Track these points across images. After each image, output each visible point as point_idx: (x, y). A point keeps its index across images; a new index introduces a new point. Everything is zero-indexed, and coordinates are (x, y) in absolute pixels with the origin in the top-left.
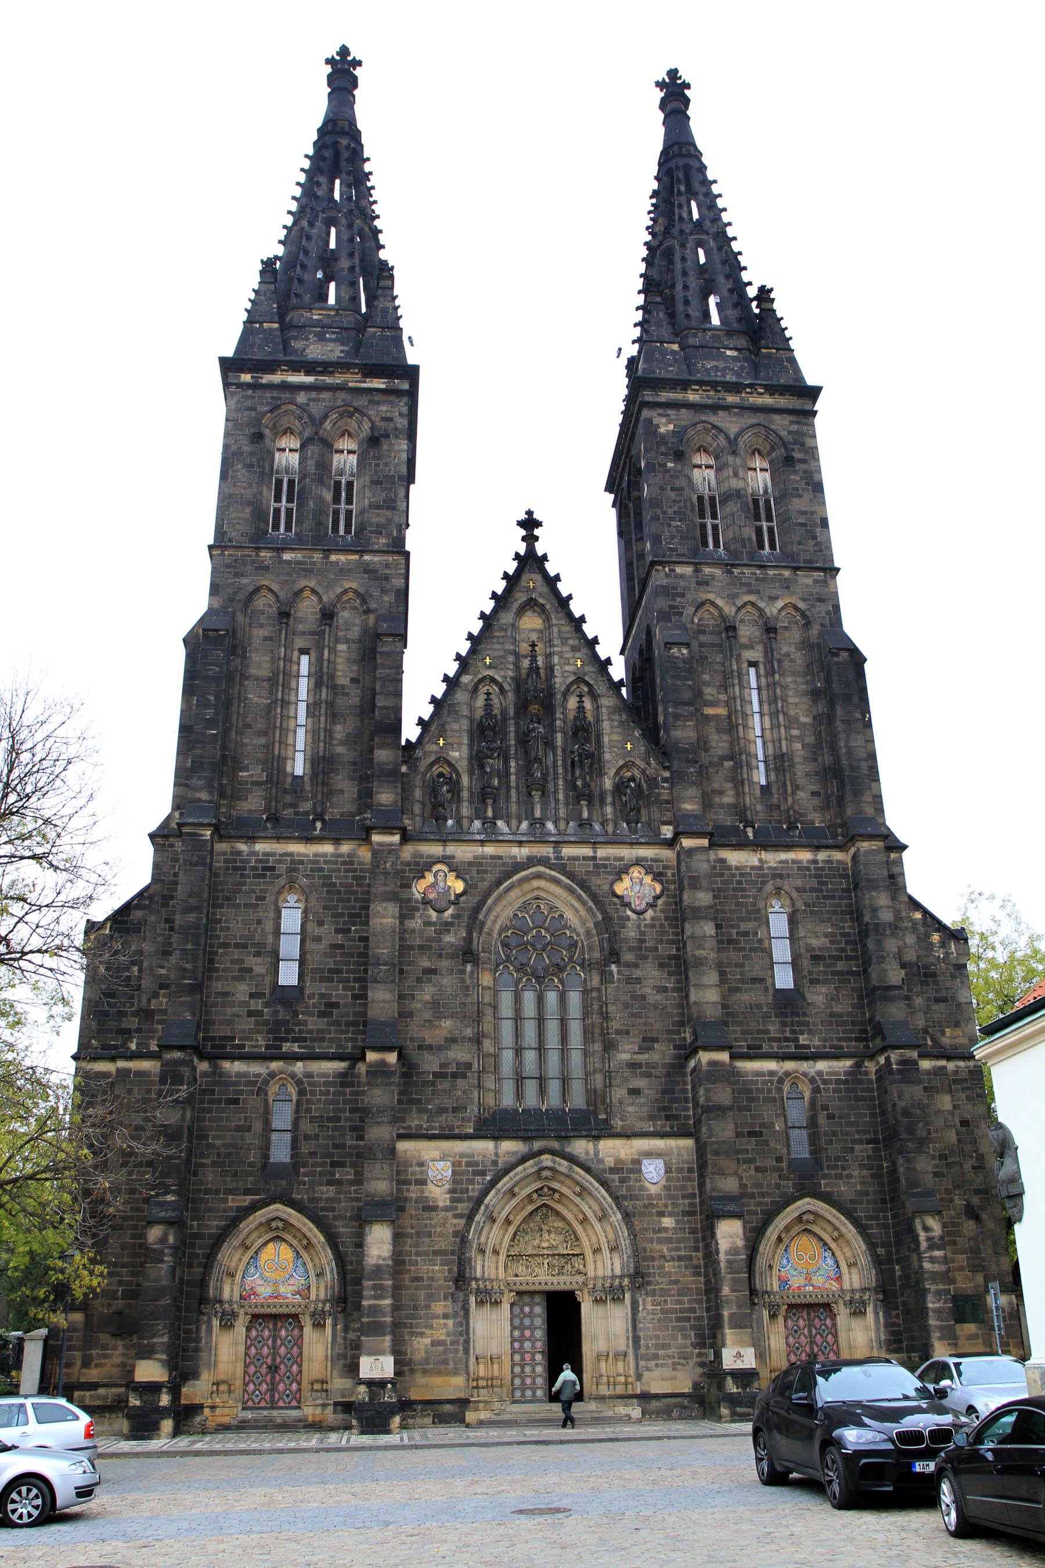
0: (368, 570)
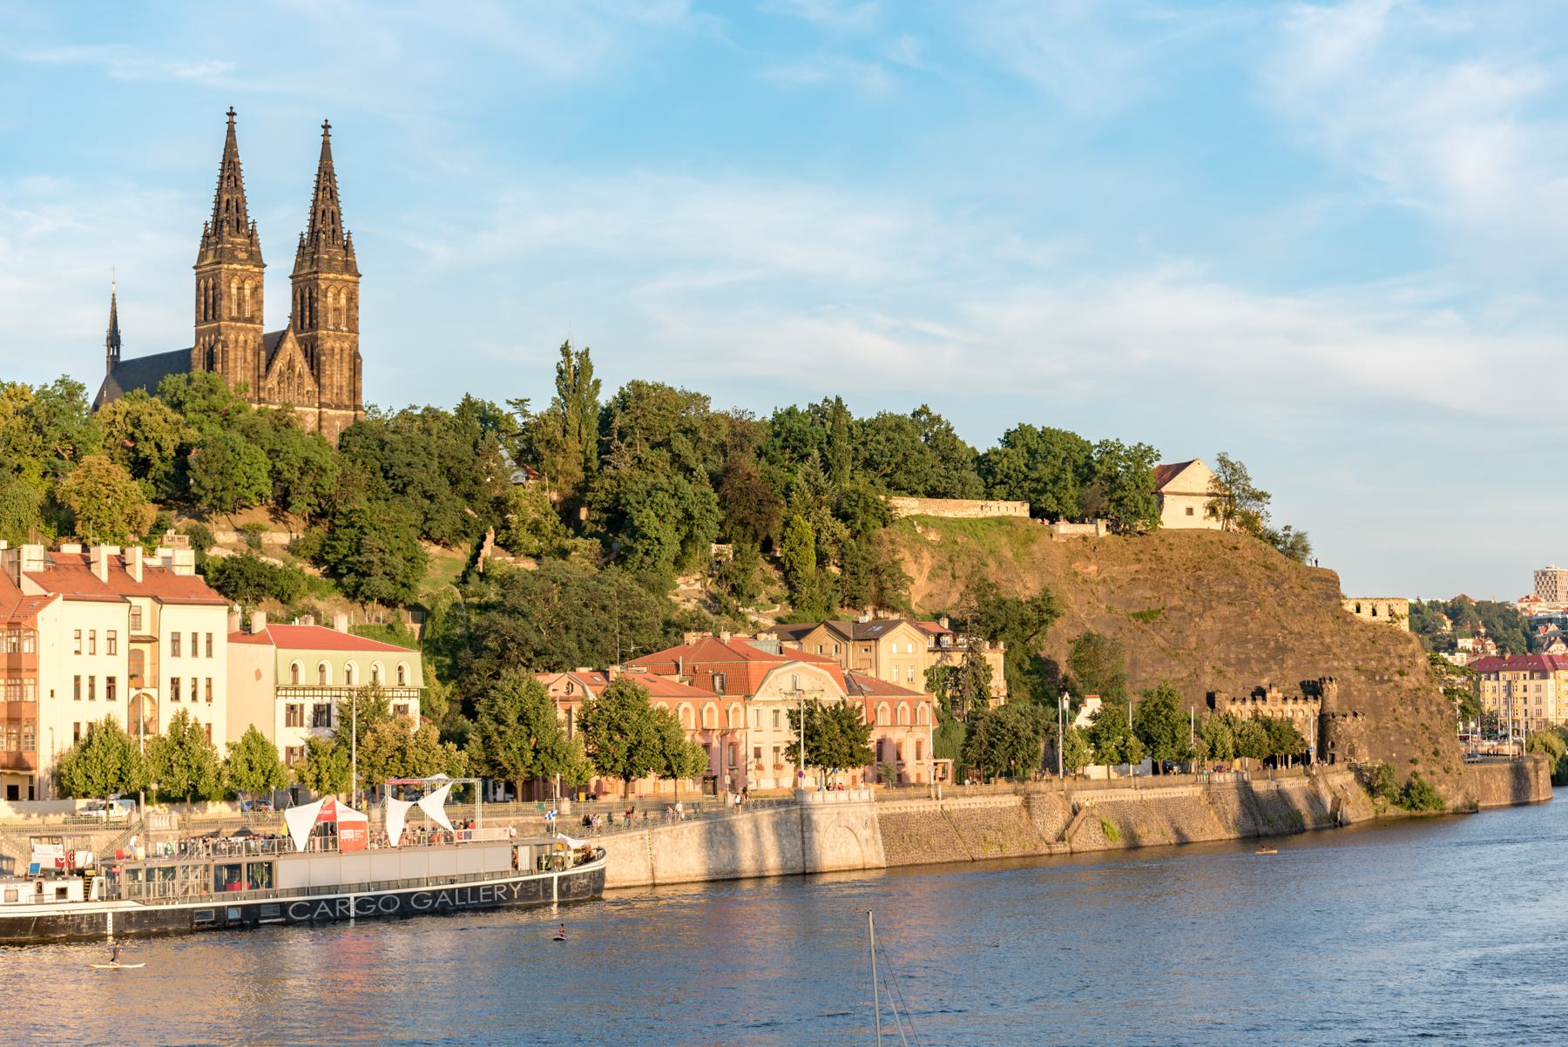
0: (255, 330)
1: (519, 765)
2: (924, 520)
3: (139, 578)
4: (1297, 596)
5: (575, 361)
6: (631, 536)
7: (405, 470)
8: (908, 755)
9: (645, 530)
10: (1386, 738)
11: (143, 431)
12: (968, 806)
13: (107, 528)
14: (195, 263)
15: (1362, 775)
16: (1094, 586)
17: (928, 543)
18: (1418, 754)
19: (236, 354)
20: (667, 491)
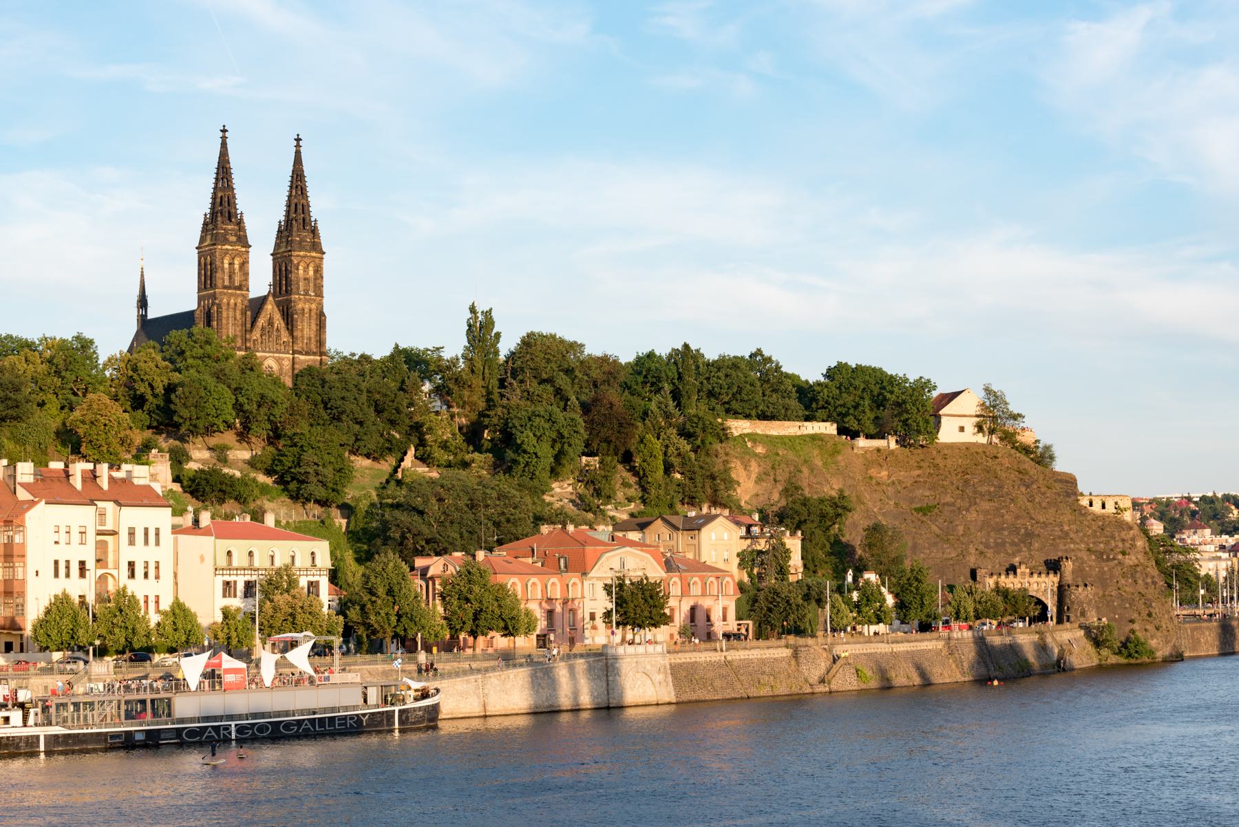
0: (243, 295)
1: (386, 626)
2: (753, 437)
3: (105, 486)
4: (1043, 494)
5: (481, 317)
6: (516, 452)
7: (339, 403)
8: (716, 616)
9: (525, 447)
10: (1111, 604)
11: (139, 375)
12: (747, 657)
13: (104, 449)
14: (197, 245)
15: (1090, 632)
16: (885, 487)
17: (756, 455)
18: (1135, 616)
19: (228, 314)
20: (543, 417)
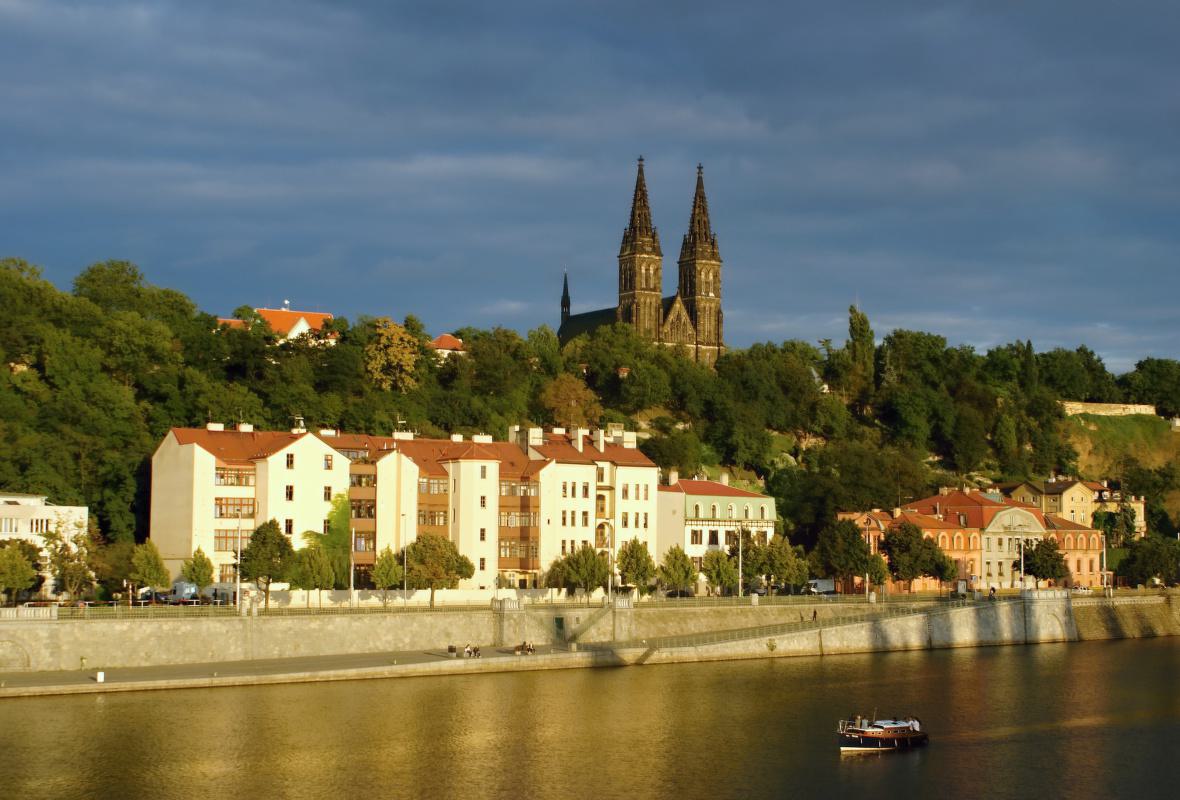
2: (1085, 416)
